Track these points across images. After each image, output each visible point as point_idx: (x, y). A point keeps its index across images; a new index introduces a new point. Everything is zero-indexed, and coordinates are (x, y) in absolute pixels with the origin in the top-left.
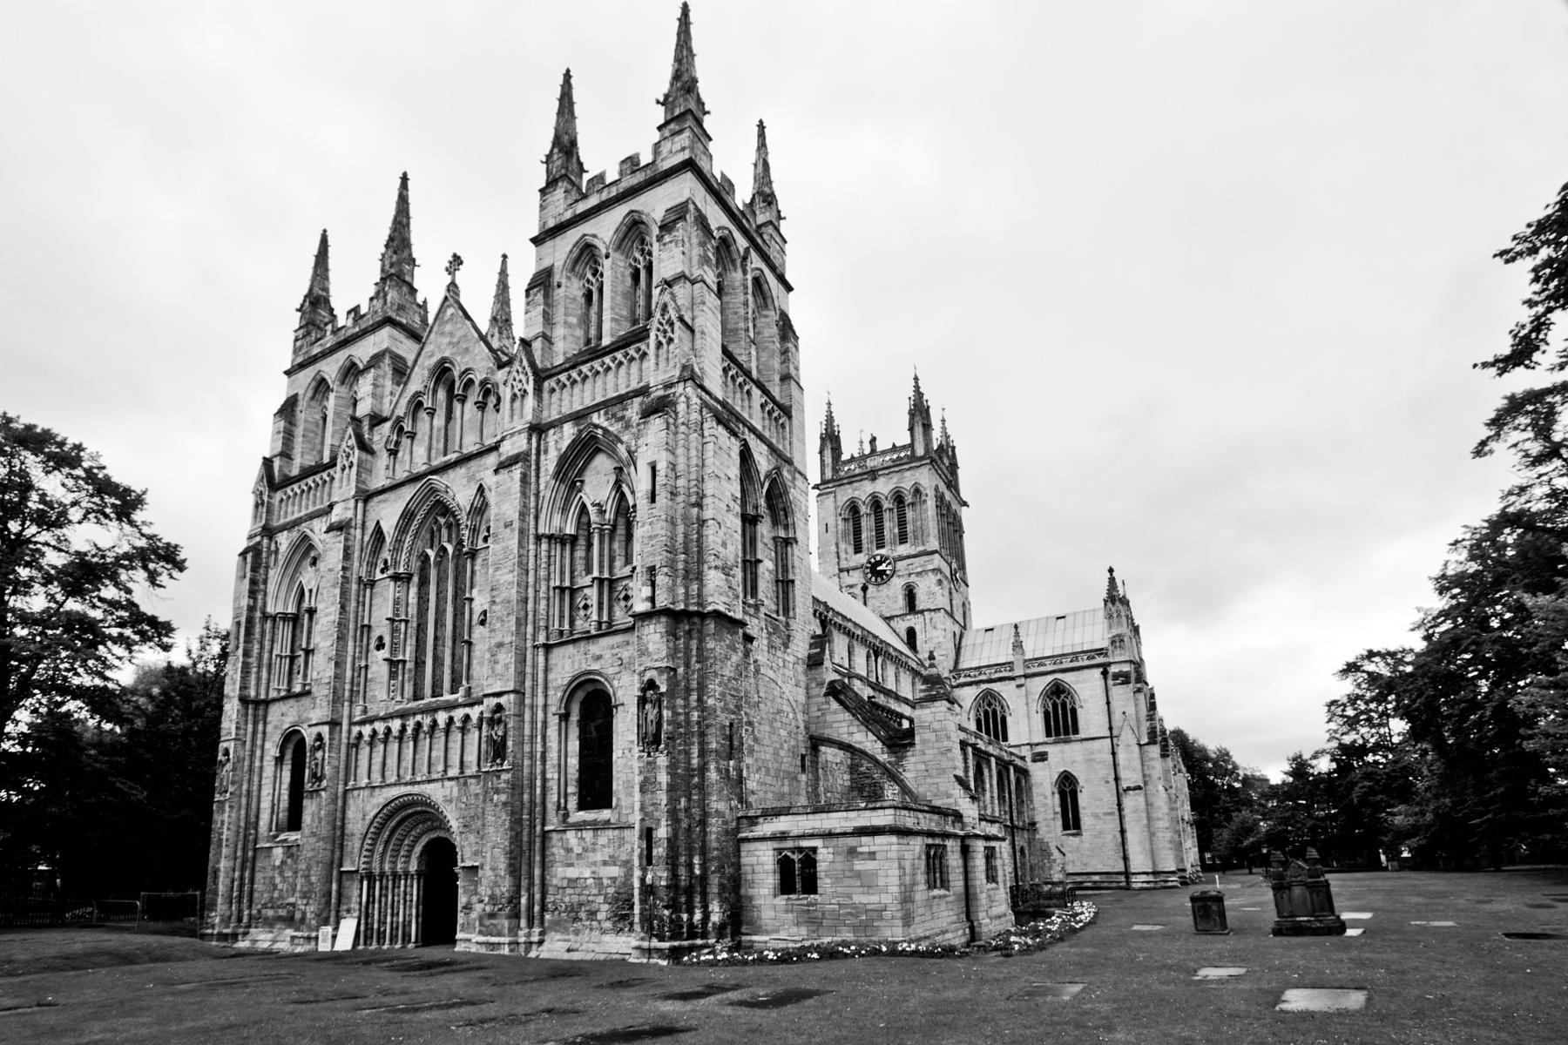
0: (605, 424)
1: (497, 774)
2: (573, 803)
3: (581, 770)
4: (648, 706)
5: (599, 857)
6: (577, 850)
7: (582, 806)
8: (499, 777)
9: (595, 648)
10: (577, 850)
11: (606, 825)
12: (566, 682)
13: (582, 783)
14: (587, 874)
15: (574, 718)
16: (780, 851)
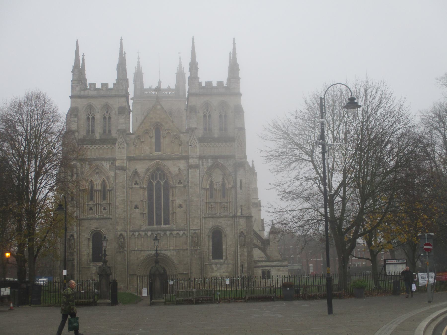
0: (222, 163)
1: (196, 250)
2: (211, 258)
3: (213, 249)
4: (241, 237)
5: (222, 271)
6: (215, 269)
7: (213, 258)
8: (197, 251)
9: (219, 220)
10: (215, 269)
11: (224, 263)
12: (210, 227)
13: (213, 253)
14: (218, 275)
15: (211, 237)
16: (262, 270)
